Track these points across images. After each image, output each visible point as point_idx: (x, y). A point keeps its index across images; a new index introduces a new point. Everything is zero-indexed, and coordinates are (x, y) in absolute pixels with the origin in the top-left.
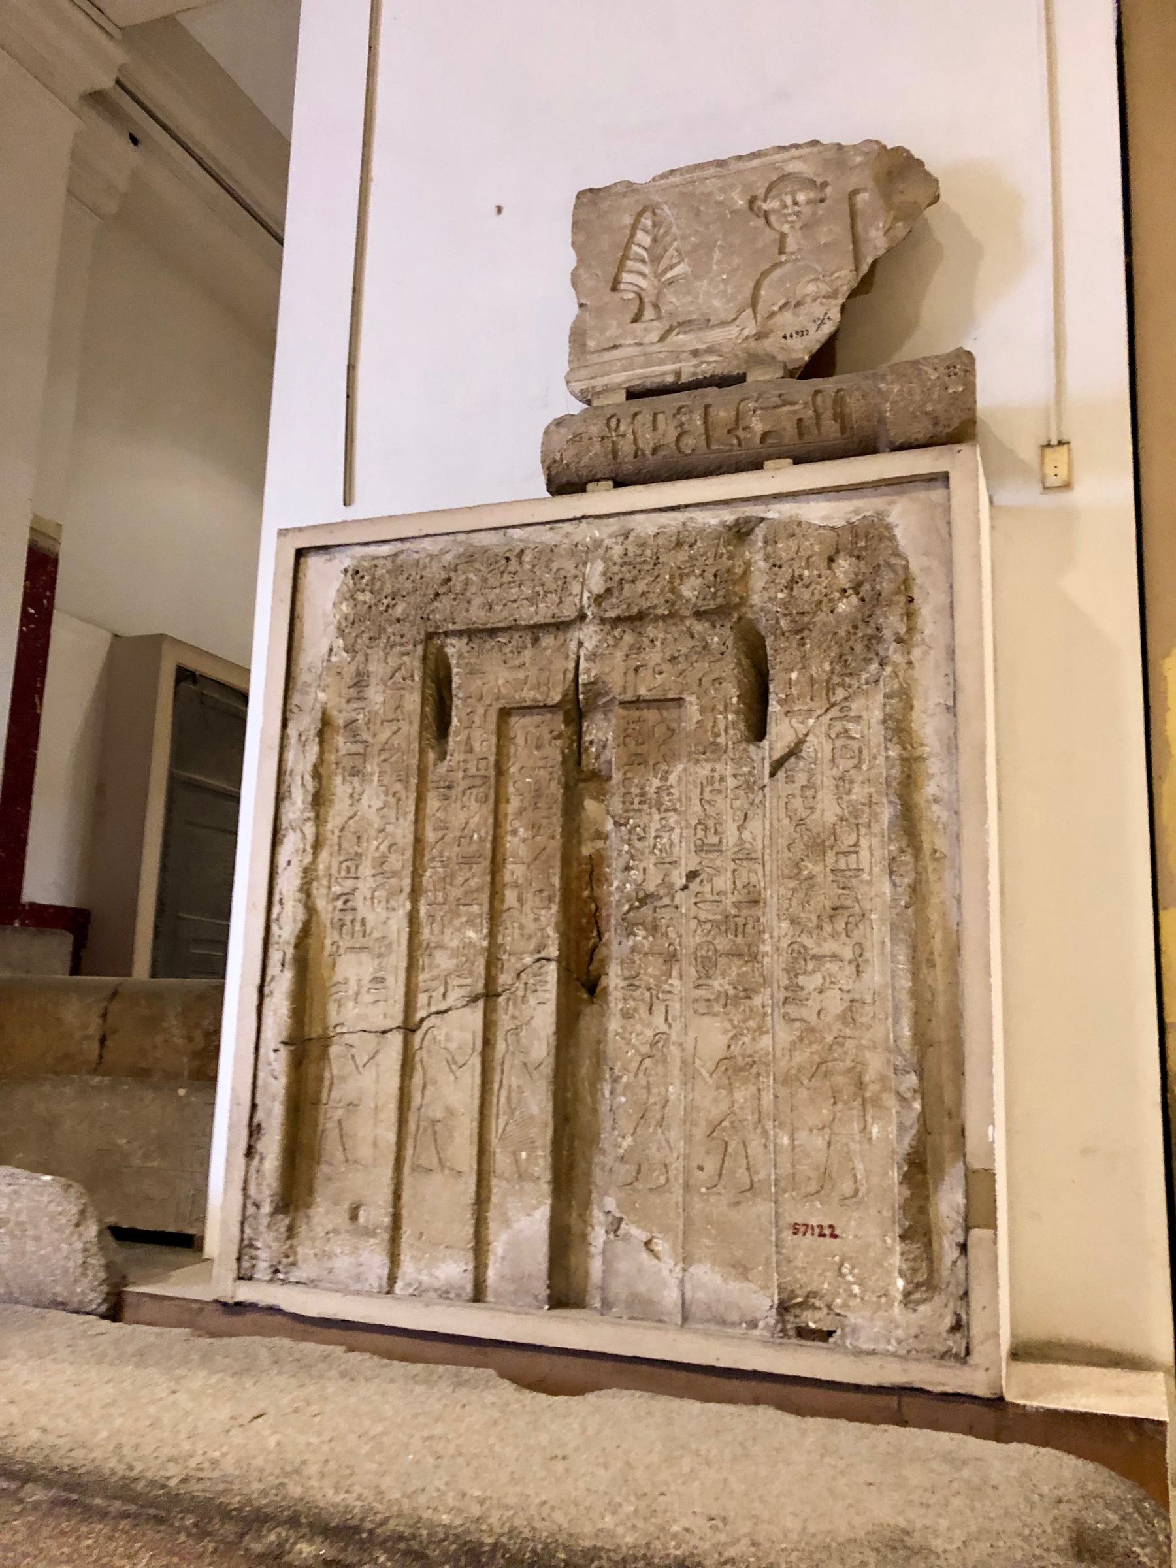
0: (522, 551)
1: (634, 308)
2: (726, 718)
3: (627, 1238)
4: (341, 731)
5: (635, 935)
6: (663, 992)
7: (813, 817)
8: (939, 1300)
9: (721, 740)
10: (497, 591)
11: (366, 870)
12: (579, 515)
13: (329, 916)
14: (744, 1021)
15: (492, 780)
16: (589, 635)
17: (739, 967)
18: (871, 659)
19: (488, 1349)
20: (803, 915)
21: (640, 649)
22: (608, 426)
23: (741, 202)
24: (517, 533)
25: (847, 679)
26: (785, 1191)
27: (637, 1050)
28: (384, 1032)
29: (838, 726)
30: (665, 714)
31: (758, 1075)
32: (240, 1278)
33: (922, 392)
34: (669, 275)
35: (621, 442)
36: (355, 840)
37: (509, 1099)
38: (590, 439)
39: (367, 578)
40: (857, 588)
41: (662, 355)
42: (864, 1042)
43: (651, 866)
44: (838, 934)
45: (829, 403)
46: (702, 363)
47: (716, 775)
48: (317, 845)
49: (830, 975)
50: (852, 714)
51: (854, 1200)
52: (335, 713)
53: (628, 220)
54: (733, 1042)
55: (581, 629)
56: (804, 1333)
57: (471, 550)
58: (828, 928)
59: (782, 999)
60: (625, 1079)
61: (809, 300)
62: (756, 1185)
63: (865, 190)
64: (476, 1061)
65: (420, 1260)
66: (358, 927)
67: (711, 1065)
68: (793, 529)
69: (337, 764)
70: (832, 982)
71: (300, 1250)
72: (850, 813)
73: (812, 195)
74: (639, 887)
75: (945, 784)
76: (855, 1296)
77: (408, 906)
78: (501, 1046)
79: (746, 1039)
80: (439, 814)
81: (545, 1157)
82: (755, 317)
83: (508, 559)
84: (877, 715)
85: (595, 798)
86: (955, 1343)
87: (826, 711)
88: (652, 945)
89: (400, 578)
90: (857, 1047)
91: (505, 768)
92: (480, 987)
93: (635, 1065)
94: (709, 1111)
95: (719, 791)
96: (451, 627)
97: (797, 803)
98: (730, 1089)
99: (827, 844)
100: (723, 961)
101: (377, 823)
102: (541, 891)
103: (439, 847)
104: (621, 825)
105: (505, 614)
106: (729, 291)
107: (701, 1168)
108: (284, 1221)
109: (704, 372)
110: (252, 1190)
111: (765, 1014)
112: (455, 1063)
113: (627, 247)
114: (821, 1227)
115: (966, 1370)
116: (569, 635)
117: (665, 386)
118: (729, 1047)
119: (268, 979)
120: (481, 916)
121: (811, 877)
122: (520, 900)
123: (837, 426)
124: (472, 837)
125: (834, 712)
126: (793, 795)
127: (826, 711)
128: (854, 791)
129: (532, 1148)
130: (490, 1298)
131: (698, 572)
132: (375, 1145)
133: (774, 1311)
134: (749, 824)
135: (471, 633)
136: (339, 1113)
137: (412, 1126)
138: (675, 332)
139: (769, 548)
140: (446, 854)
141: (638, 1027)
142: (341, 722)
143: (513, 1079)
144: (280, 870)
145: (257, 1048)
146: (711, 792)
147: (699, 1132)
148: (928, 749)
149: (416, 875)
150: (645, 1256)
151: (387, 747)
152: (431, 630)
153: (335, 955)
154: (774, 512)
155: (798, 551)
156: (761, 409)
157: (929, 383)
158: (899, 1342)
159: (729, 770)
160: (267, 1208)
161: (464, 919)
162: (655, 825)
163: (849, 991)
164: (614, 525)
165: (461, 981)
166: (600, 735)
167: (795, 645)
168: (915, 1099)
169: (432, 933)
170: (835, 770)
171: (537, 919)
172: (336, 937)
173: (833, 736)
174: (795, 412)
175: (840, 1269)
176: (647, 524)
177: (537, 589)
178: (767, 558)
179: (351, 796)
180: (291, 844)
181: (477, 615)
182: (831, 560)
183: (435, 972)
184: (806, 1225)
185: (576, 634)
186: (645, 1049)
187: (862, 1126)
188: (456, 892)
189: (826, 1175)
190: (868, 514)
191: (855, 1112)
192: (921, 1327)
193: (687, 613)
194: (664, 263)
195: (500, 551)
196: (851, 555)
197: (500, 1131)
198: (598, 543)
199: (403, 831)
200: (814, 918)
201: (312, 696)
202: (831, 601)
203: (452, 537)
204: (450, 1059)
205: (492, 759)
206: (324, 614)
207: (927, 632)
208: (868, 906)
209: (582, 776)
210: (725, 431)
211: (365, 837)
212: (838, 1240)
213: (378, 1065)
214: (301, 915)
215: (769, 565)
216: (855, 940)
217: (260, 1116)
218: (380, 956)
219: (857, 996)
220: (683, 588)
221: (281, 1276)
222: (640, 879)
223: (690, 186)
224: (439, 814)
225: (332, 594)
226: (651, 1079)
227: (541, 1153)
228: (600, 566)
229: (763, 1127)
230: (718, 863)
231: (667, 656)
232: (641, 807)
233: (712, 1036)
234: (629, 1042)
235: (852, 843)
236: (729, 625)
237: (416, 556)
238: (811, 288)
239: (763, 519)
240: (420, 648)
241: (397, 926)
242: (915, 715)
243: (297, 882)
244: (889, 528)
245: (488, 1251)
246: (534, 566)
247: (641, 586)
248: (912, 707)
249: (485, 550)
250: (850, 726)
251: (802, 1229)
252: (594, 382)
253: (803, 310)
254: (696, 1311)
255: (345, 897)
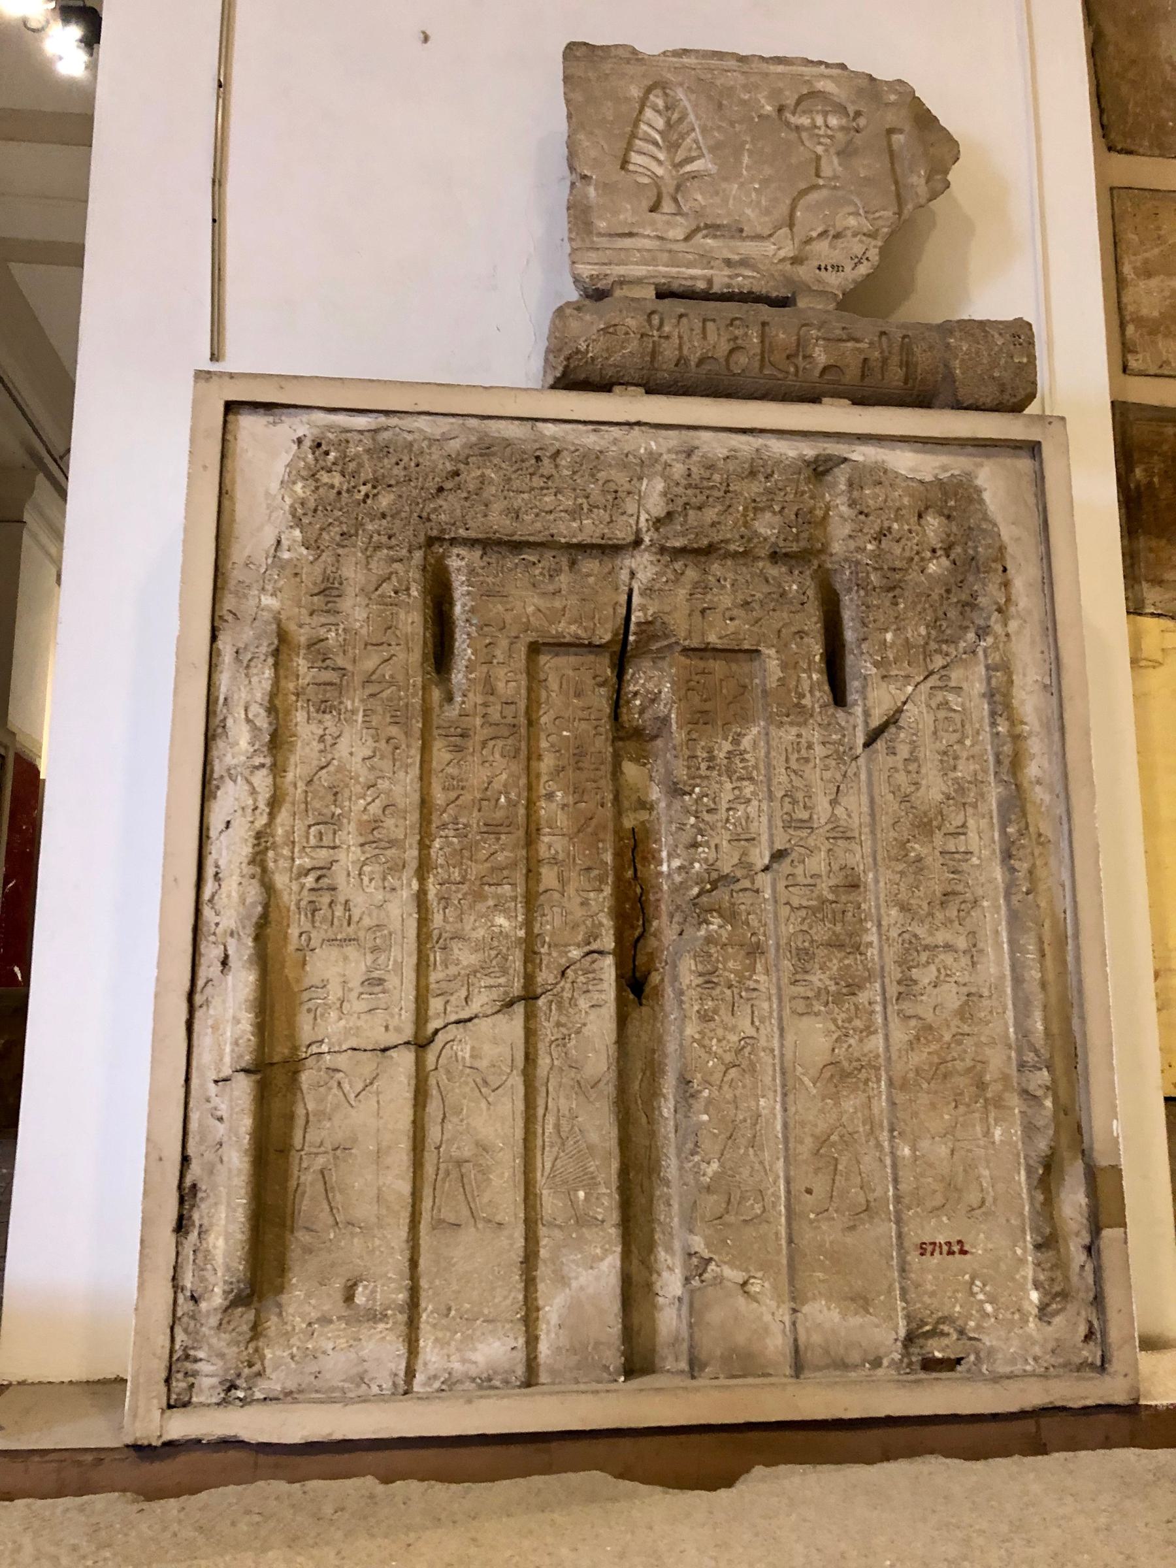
0: (558, 452)
1: (652, 195)
2: (810, 677)
3: (719, 1280)
4: (302, 652)
5: (708, 923)
6: (748, 989)
7: (919, 794)
8: (1071, 1308)
9: (806, 701)
10: (526, 496)
11: (349, 836)
12: (633, 420)
13: (294, 898)
14: (850, 1020)
15: (523, 731)
16: (643, 567)
17: (841, 961)
18: (967, 627)
19: (554, 1445)
20: (912, 901)
21: (707, 589)
22: (649, 320)
23: (769, 108)
24: (549, 429)
25: (944, 647)
26: (909, 1209)
27: (720, 1058)
28: (384, 1050)
29: (939, 696)
30: (734, 666)
31: (867, 1080)
32: (170, 1407)
33: (989, 355)
34: (688, 168)
35: (665, 344)
36: (331, 798)
37: (557, 1126)
38: (627, 333)
39: (332, 455)
40: (947, 551)
41: (690, 257)
42: (983, 1039)
43: (724, 843)
44: (951, 922)
45: (896, 349)
46: (738, 275)
47: (803, 741)
48: (275, 803)
49: (945, 968)
50: (953, 684)
51: (983, 1209)
52: (292, 627)
53: (635, 92)
54: (838, 1045)
55: (633, 556)
56: (930, 1365)
57: (488, 441)
58: (939, 916)
59: (895, 995)
60: (706, 1093)
61: (849, 233)
62: (872, 1204)
63: (901, 131)
64: (517, 1081)
65: (448, 1344)
66: (339, 911)
67: (814, 1072)
68: (880, 476)
69: (297, 695)
70: (947, 975)
71: (268, 1353)
72: (955, 791)
73: (844, 121)
74: (711, 867)
75: (1046, 765)
76: (988, 1315)
77: (415, 885)
78: (544, 1062)
79: (852, 1041)
80: (450, 770)
81: (610, 1195)
82: (793, 239)
83: (538, 458)
84: (979, 687)
85: (636, 760)
86: (1091, 1352)
87: (925, 678)
88: (731, 935)
89: (386, 461)
90: (976, 1045)
91: (534, 717)
92: (517, 988)
93: (718, 1076)
94: (816, 1126)
95: (807, 760)
96: (462, 532)
97: (901, 778)
98: (836, 1097)
99: (935, 823)
100: (821, 952)
101: (364, 775)
102: (589, 869)
103: (451, 810)
104: (685, 793)
105: (538, 525)
106: (763, 202)
107: (809, 1191)
108: (244, 1318)
109: (740, 286)
110: (188, 1281)
111: (873, 1012)
112: (486, 1083)
113: (636, 124)
114: (949, 1244)
115: (1107, 1378)
116: (618, 562)
117: (693, 292)
118: (833, 1050)
119: (200, 983)
120: (515, 899)
121: (919, 859)
122: (561, 879)
123: (901, 373)
124: (498, 800)
125: (933, 681)
126: (896, 769)
127: (925, 678)
128: (960, 767)
129: (591, 1185)
130: (544, 1377)
131: (777, 508)
132: (379, 1198)
133: (899, 1344)
134: (843, 800)
135: (487, 544)
136: (321, 1161)
137: (429, 1169)
138: (700, 235)
139: (856, 494)
140: (463, 820)
141: (720, 1032)
142: (303, 640)
143: (562, 1101)
144: (213, 833)
145: (187, 1080)
146: (797, 760)
147: (805, 1149)
148: (1027, 728)
149: (424, 846)
150: (741, 1300)
151: (374, 677)
152: (435, 533)
153: (305, 950)
154: (860, 454)
155: (886, 501)
156: (824, 339)
157: (996, 349)
158: (1035, 1359)
159: (817, 737)
160: (217, 1299)
161: (491, 903)
162: (726, 796)
163: (965, 985)
164: (673, 439)
165: (491, 981)
166: (650, 686)
167: (888, 604)
168: (1046, 1097)
169: (445, 920)
170: (938, 743)
171: (585, 903)
172: (307, 926)
173: (934, 706)
174: (860, 351)
175: (971, 1288)
176: (715, 445)
177: (580, 501)
178: (852, 504)
179: (322, 739)
180: (230, 799)
181: (498, 522)
182: (920, 516)
183: (453, 970)
184: (934, 1244)
185: (629, 561)
186: (729, 1058)
187: (985, 1129)
188: (475, 870)
189: (952, 1187)
190: (956, 473)
191: (977, 1115)
192: (1057, 1340)
193: (763, 553)
194: (680, 156)
195: (528, 447)
196: (941, 514)
197: (548, 1165)
198: (654, 458)
199: (404, 786)
200: (925, 906)
201: (252, 602)
202: (922, 559)
203: (460, 421)
204: (479, 1080)
205: (522, 705)
206: (267, 494)
207: (1022, 605)
208: (980, 892)
209: (621, 734)
210: (784, 356)
211: (346, 793)
212: (968, 1257)
213: (378, 1093)
214: (254, 892)
215: (856, 512)
216: (969, 929)
217: (195, 1170)
218: (375, 949)
219: (973, 990)
220: (756, 523)
221: (241, 1394)
222: (712, 856)
223: (714, 77)
224: (450, 770)
225: (279, 468)
226: (737, 1093)
227: (604, 1190)
228: (660, 485)
229: (876, 1138)
230: (811, 842)
231: (739, 601)
232: (708, 773)
233: (814, 1038)
234: (709, 1052)
235: (960, 824)
236: (808, 573)
237: (410, 437)
238: (852, 222)
239: (845, 460)
240: (418, 555)
241: (399, 911)
242: (1015, 691)
243: (247, 850)
244: (979, 491)
245: (537, 1318)
246: (574, 473)
247: (710, 514)
248: (1012, 682)
249: (507, 443)
250: (951, 697)
251: (930, 1248)
252: (607, 270)
253: (840, 243)
254: (808, 1356)
255: (319, 873)
